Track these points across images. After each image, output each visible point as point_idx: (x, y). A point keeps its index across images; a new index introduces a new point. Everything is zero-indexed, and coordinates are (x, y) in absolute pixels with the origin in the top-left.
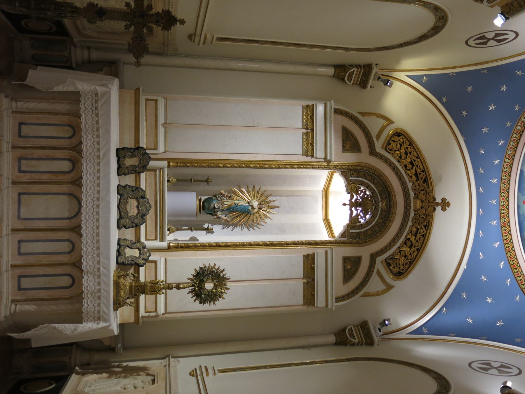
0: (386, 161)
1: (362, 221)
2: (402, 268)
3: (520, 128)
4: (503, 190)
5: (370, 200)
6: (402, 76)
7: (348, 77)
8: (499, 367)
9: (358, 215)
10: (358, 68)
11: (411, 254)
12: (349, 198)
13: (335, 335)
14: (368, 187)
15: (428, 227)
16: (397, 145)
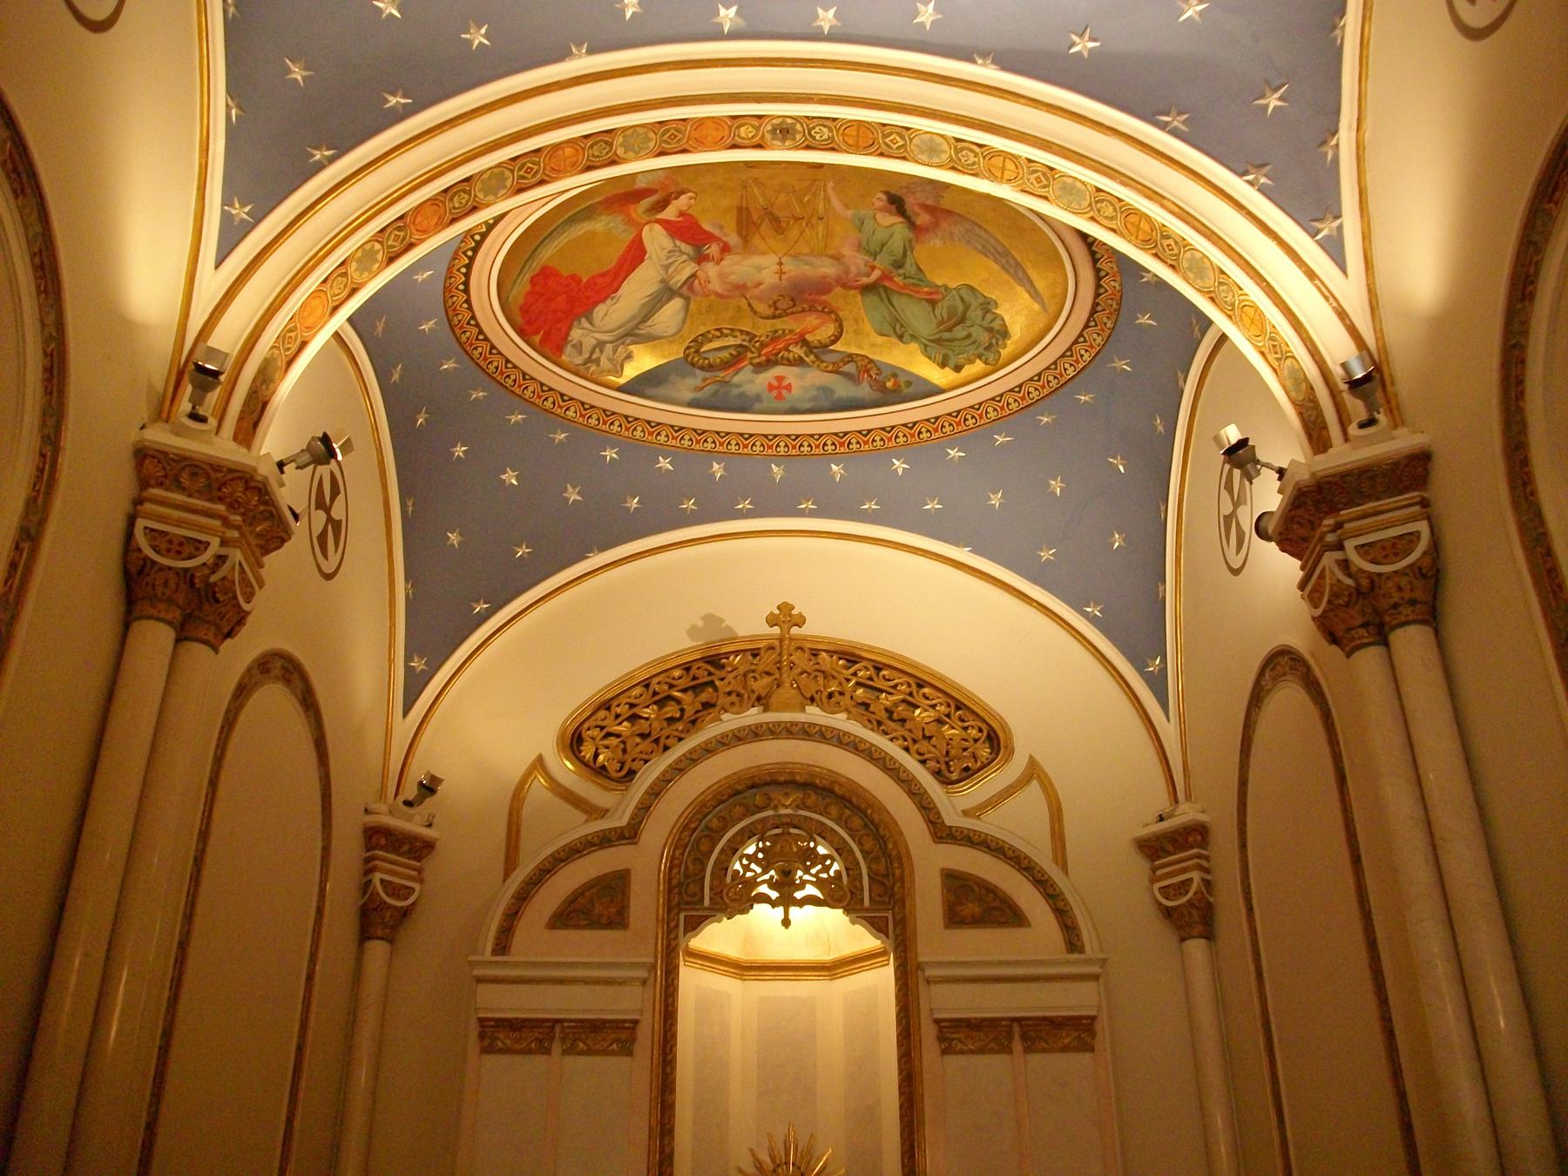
0: (656, 792)
1: (836, 866)
2: (973, 732)
4: (746, 446)
5: (774, 844)
6: (404, 728)
7: (399, 898)
9: (819, 883)
10: (373, 870)
12: (766, 907)
13: (1183, 940)
14: (733, 849)
15: (853, 655)
16: (607, 747)
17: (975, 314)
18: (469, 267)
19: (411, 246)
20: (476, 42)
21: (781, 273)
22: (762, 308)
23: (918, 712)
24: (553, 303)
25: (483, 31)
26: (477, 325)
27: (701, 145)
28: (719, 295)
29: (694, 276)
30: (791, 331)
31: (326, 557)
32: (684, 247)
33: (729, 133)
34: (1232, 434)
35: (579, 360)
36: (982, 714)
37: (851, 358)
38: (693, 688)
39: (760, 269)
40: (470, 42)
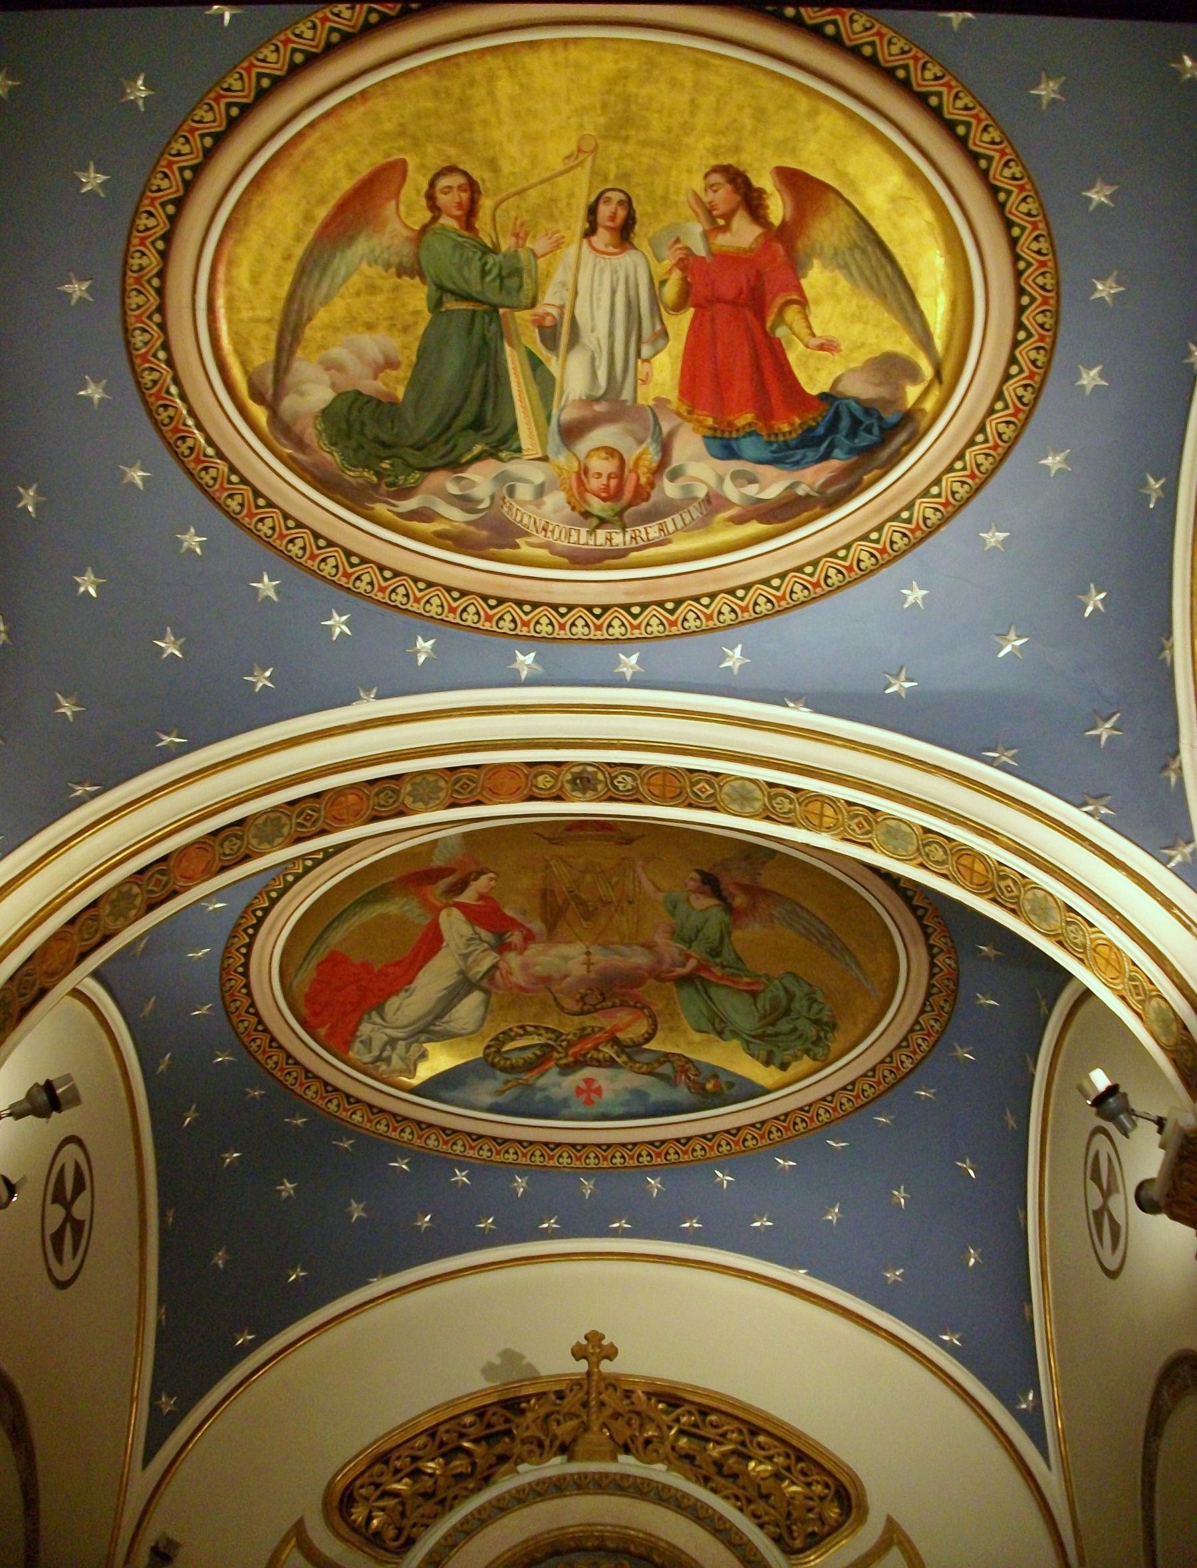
2: (818, 1489)
3: (359, 1113)
4: (551, 1158)
8: (1100, 1187)
11: (770, 1458)
16: (383, 1509)
17: (799, 1005)
18: (249, 946)
19: (175, 894)
20: (260, 685)
21: (589, 964)
22: (569, 1004)
23: (752, 1464)
24: (341, 992)
25: (268, 674)
26: (257, 1014)
27: (495, 795)
28: (521, 988)
29: (495, 967)
30: (601, 1029)
31: (60, 1259)
32: (485, 934)
33: (525, 781)
34: (1100, 1080)
35: (367, 1058)
36: (828, 1465)
37: (667, 1057)
38: (487, 1438)
39: (566, 959)
40: (254, 684)
